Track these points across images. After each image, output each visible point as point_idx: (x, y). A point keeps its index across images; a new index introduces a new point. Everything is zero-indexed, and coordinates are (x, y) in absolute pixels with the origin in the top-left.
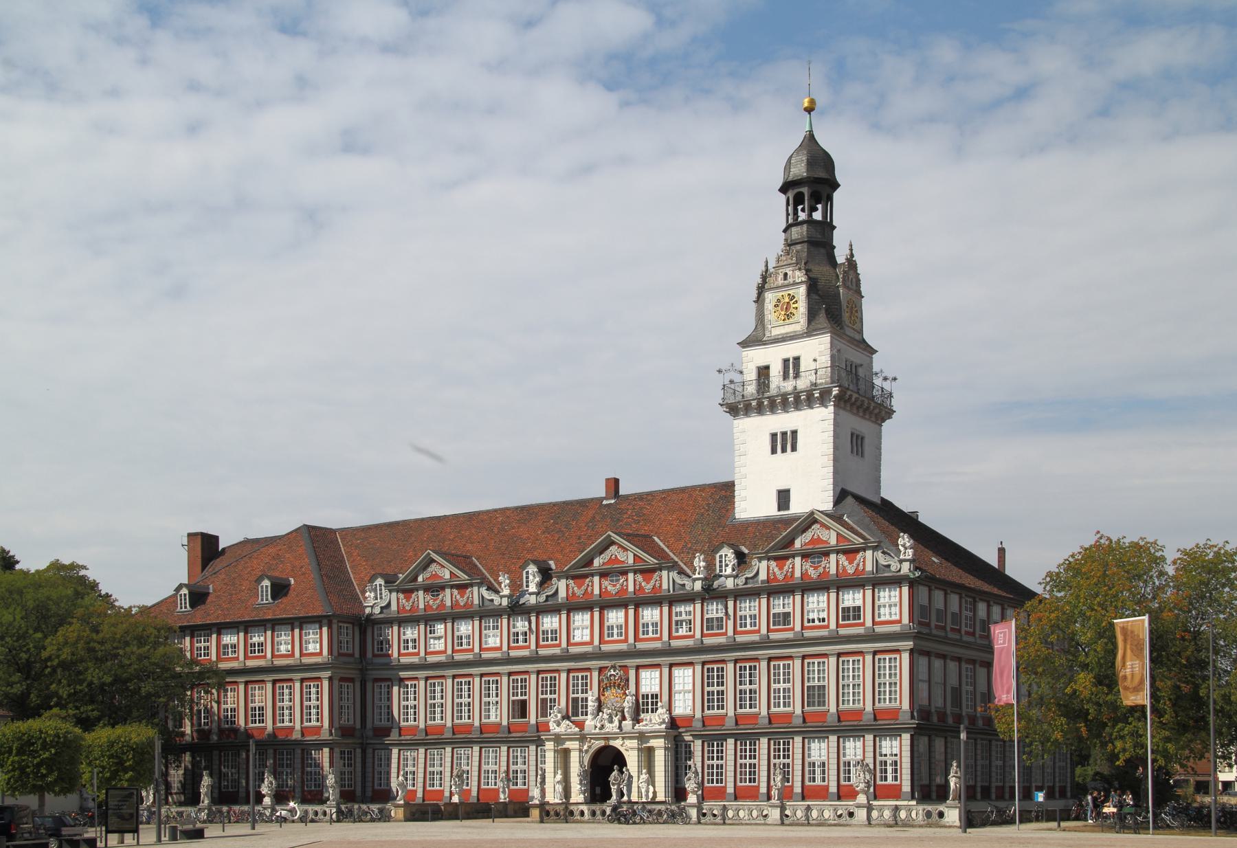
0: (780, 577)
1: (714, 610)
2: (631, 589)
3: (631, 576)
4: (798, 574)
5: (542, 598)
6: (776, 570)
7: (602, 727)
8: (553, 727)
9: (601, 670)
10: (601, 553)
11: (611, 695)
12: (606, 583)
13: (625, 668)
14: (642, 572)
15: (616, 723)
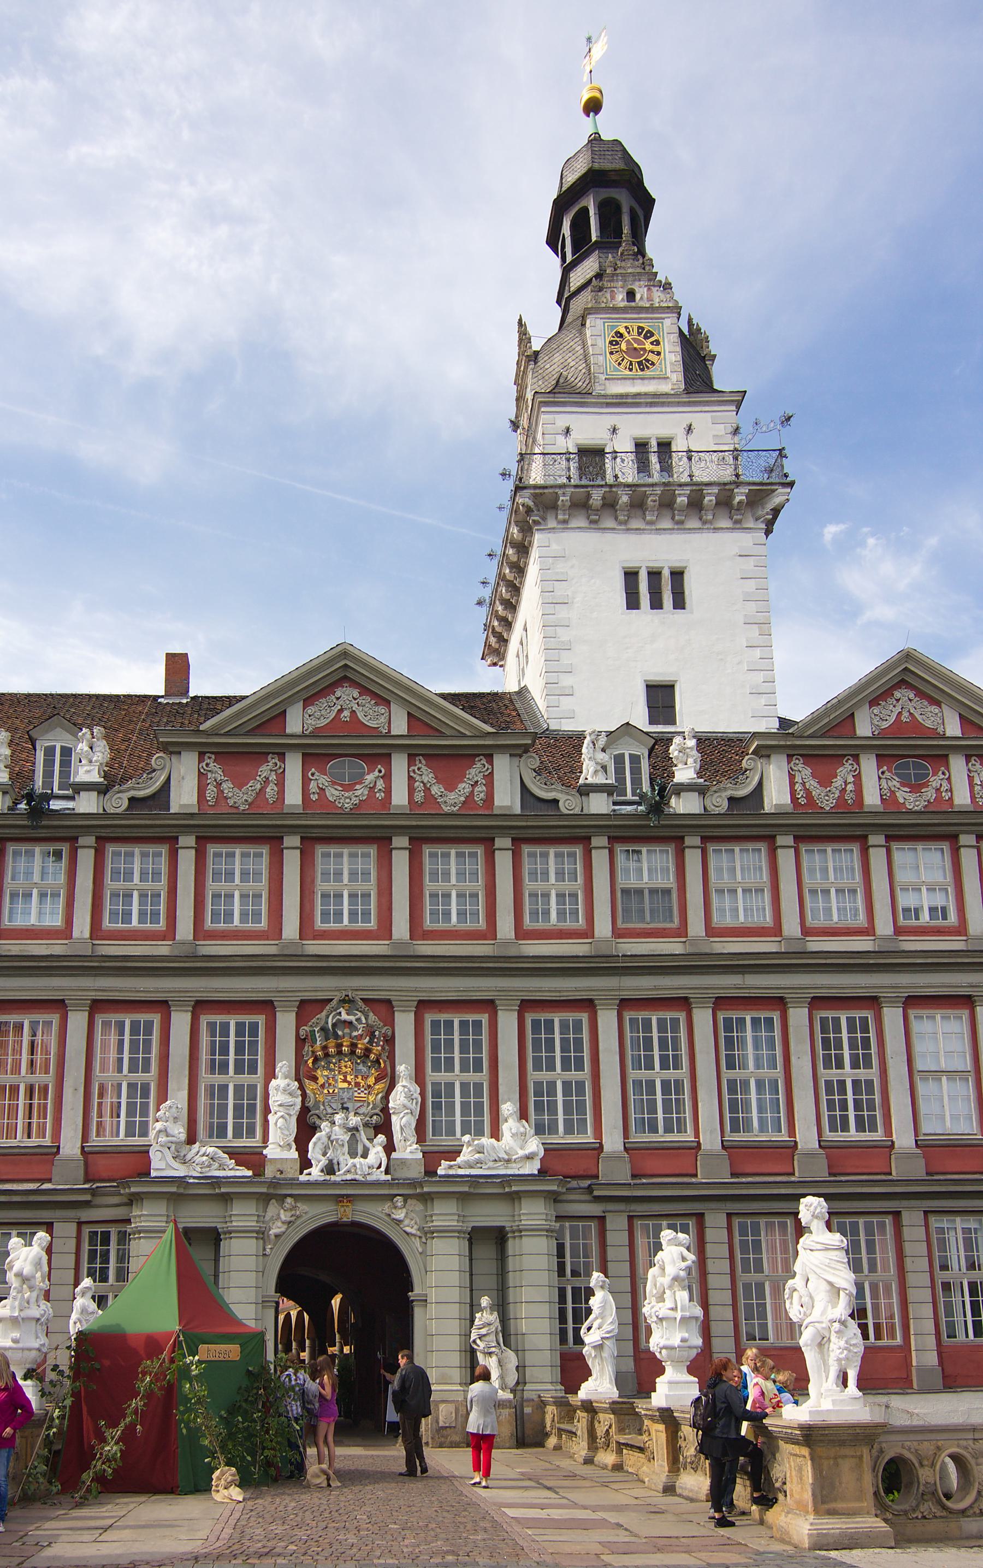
0: (828, 803)
1: (650, 868)
2: (400, 797)
3: (399, 765)
4: (872, 798)
5: (118, 802)
6: (812, 784)
7: (330, 1169)
8: (162, 1164)
9: (307, 1008)
10: (308, 702)
11: (339, 1079)
12: (320, 780)
13: (385, 1007)
14: (434, 757)
15: (377, 1153)
